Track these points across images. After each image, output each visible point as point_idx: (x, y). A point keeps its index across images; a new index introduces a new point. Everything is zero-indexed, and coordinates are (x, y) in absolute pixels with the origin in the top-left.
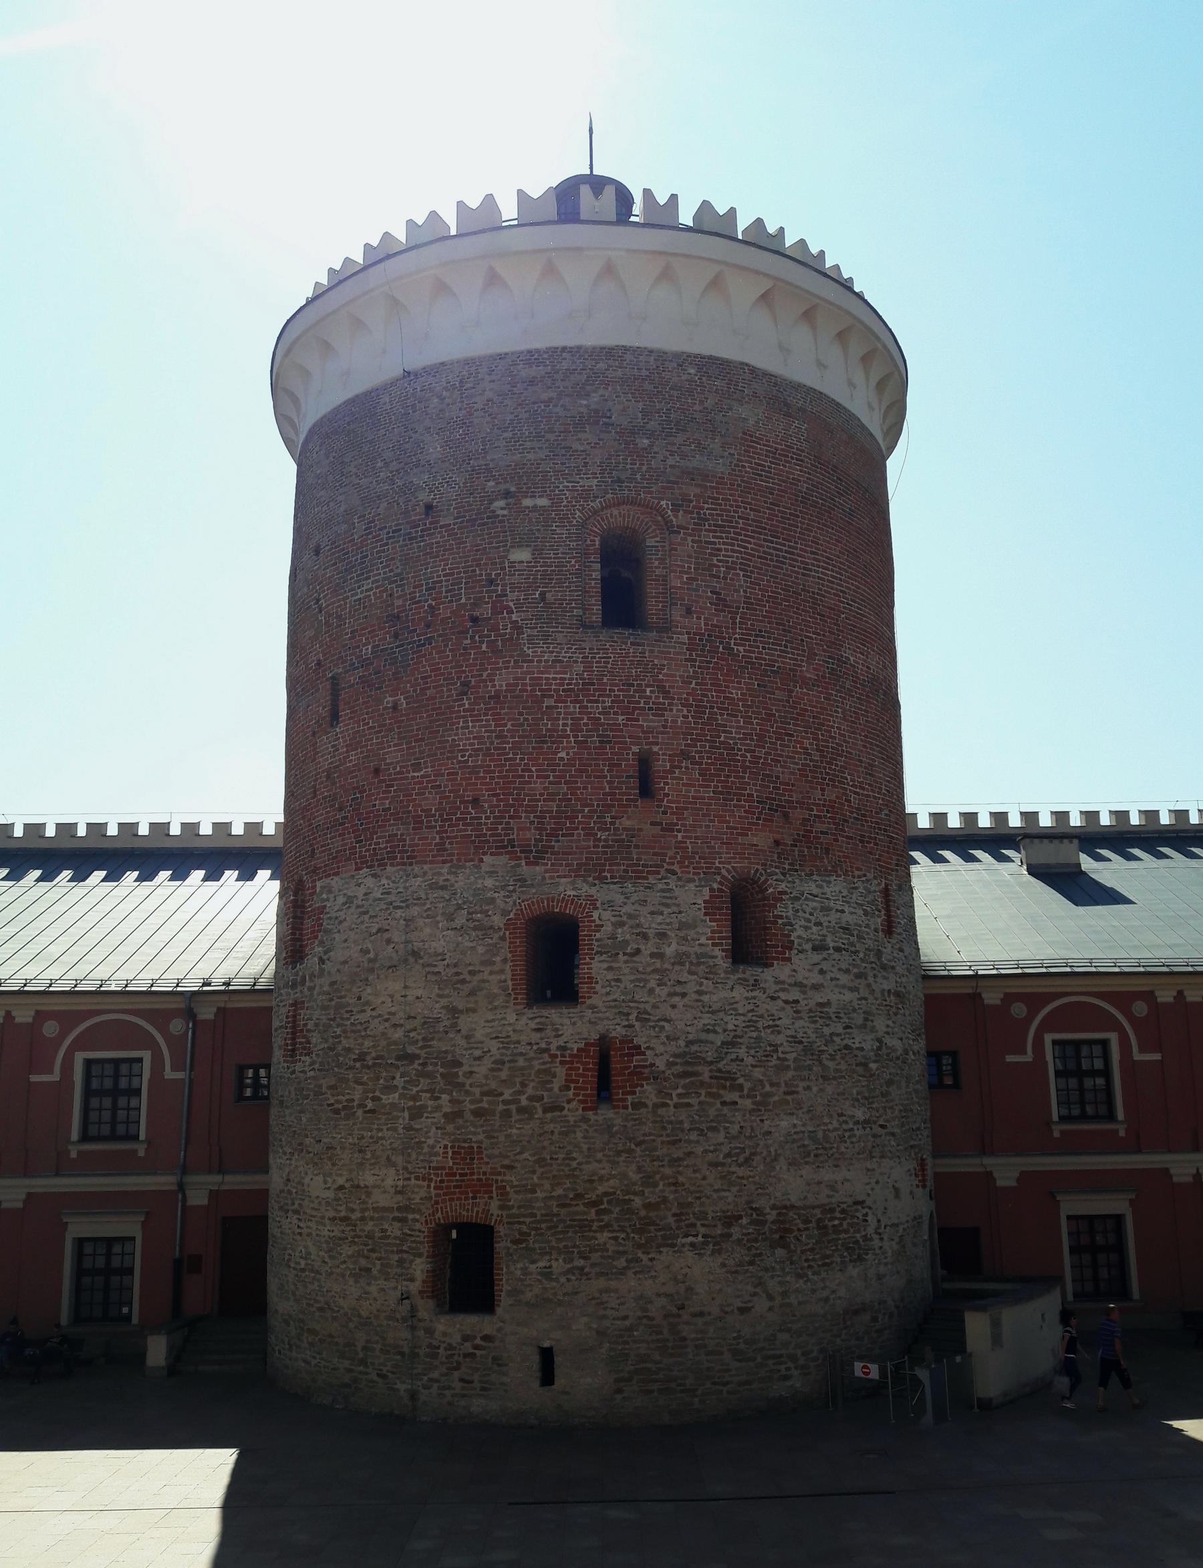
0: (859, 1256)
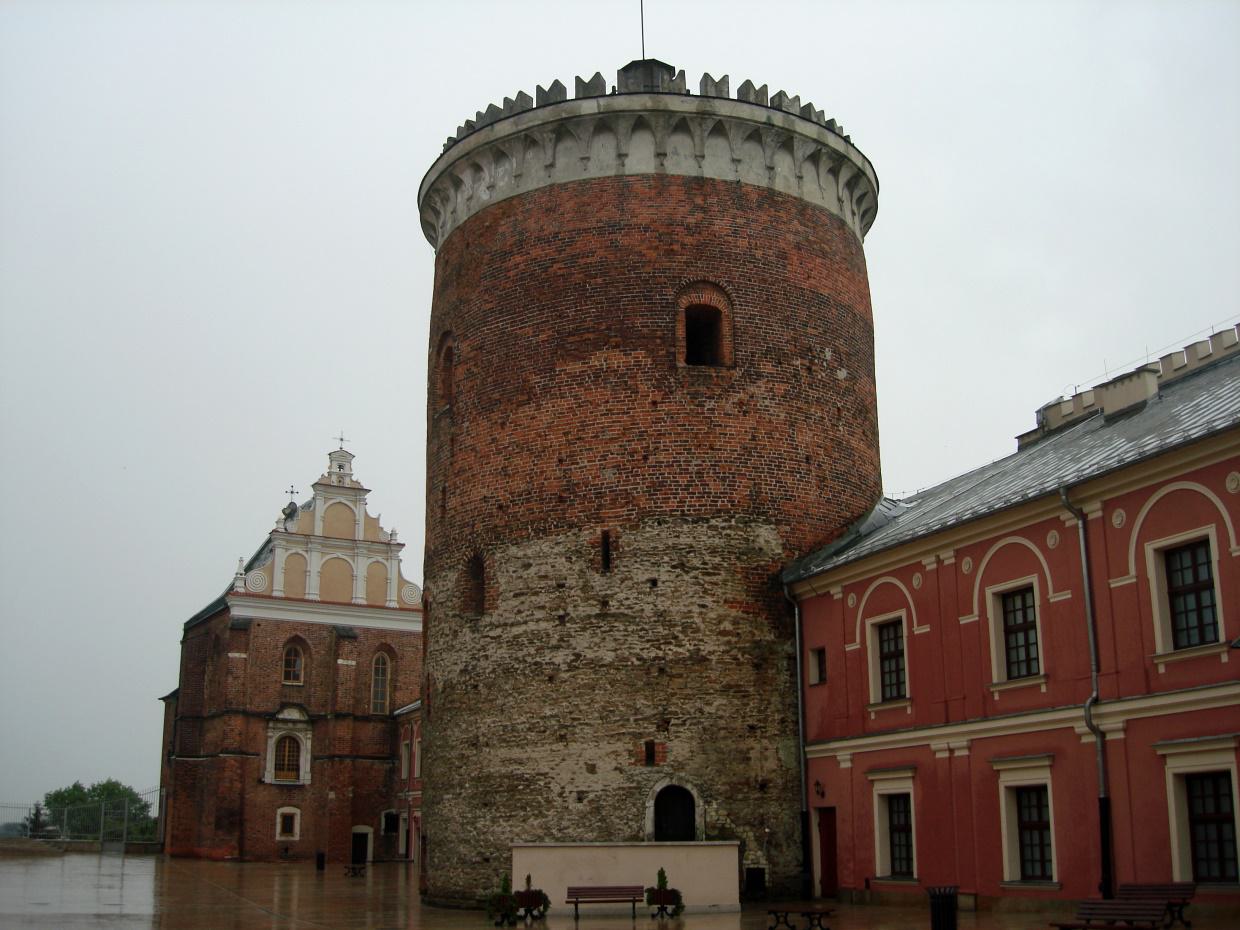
0: (540, 812)
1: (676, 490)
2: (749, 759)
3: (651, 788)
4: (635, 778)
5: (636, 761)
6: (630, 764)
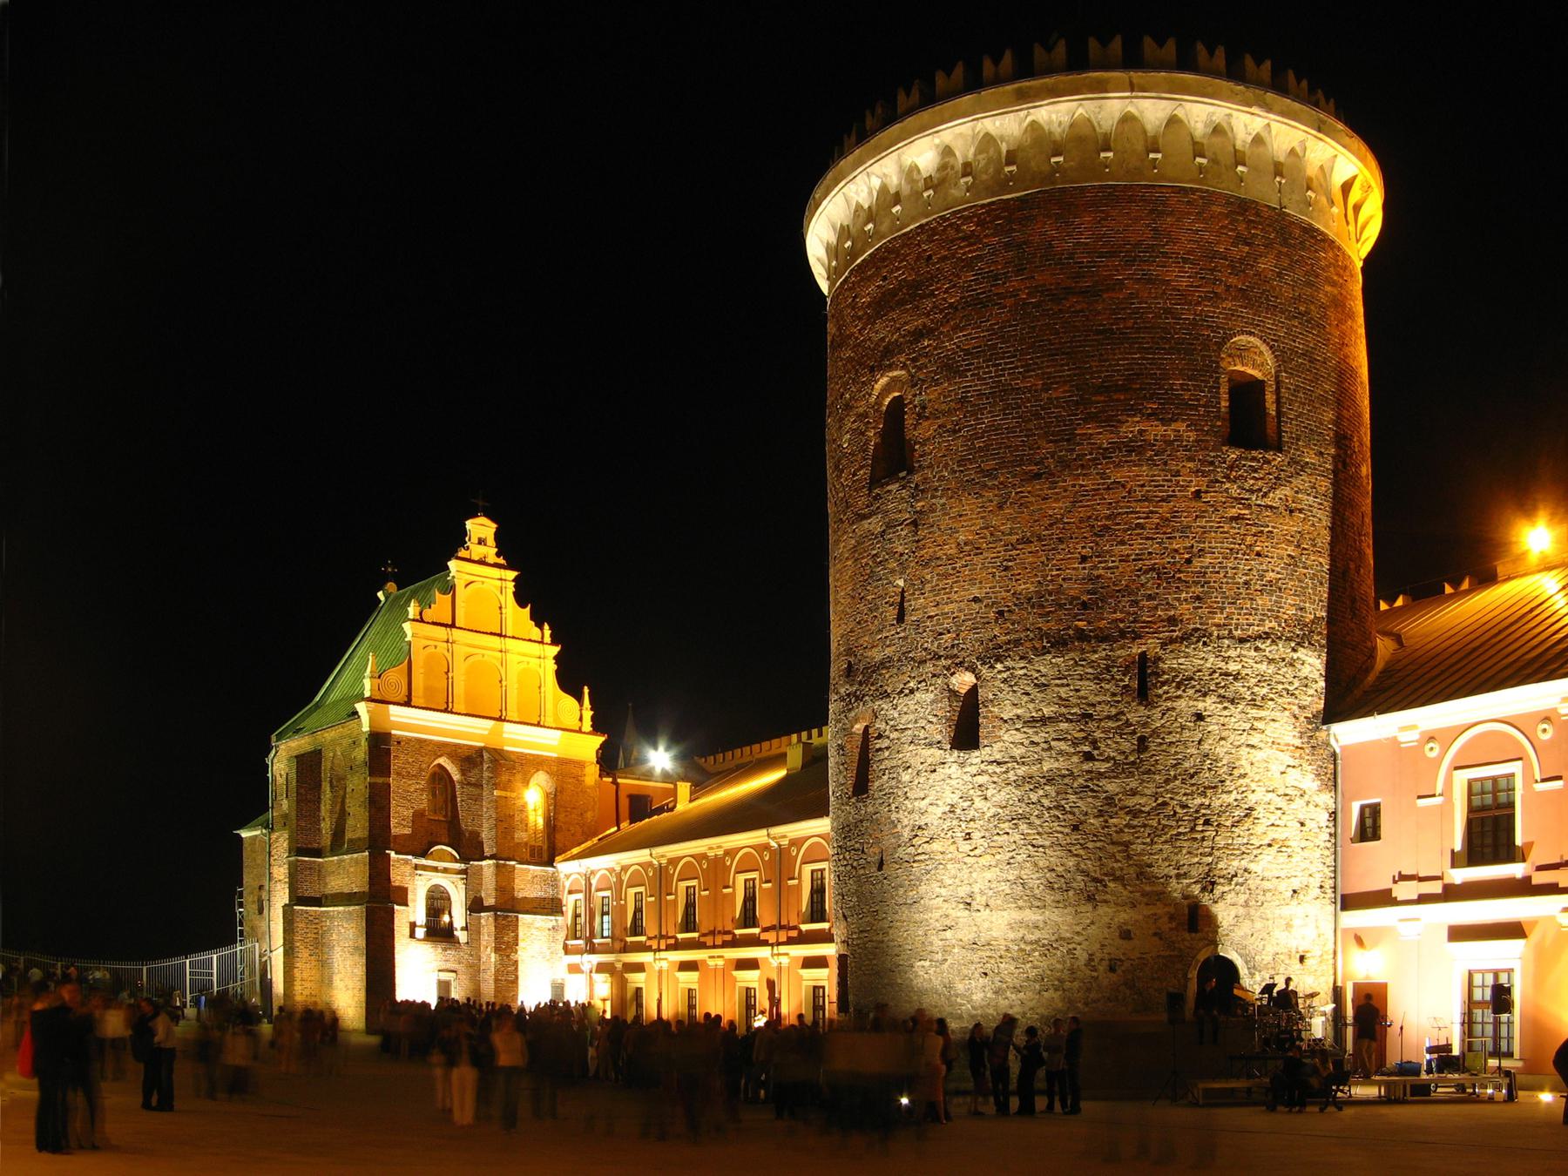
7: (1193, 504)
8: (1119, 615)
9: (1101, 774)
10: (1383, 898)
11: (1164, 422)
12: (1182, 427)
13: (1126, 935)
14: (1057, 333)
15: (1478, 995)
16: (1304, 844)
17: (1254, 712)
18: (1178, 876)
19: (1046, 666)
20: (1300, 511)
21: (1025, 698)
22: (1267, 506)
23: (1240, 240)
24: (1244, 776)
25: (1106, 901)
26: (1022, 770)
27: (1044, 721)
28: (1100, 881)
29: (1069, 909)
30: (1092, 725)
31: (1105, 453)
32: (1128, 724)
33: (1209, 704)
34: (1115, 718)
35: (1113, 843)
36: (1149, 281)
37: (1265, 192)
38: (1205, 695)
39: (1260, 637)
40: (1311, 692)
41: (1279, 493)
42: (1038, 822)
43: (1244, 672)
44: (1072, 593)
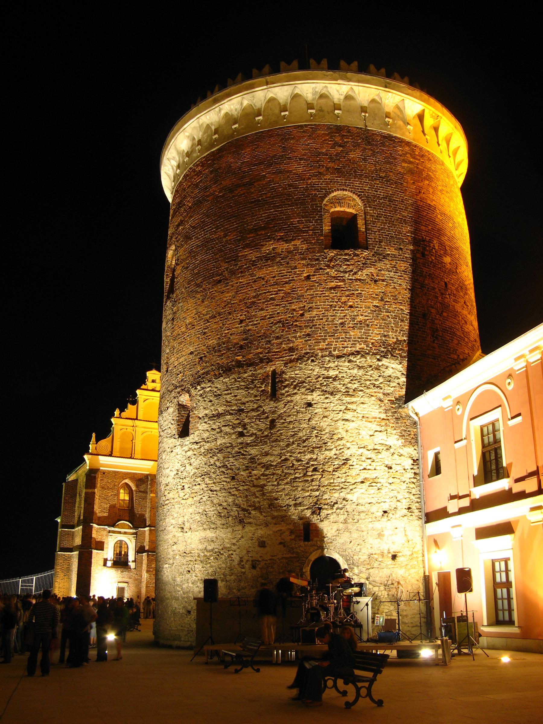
1: (325, 336)
2: (383, 535)
3: (307, 558)
4: (295, 550)
5: (296, 536)
6: (291, 540)
7: (305, 282)
8: (259, 350)
9: (247, 444)
10: (442, 514)
11: (287, 241)
12: (298, 243)
13: (262, 544)
14: (231, 207)
15: (498, 580)
16: (391, 480)
17: (348, 399)
18: (295, 505)
19: (220, 384)
20: (383, 281)
21: (210, 404)
22: (356, 280)
23: (336, 144)
24: (341, 439)
25: (250, 523)
26: (207, 446)
27: (219, 415)
28: (247, 510)
29: (230, 529)
30: (243, 415)
31: (254, 263)
32: (264, 412)
33: (315, 397)
34: (256, 410)
35: (254, 486)
36: (280, 172)
37: (355, 121)
38: (312, 391)
39: (353, 354)
40: (392, 384)
41: (365, 272)
42: (214, 476)
43: (340, 376)
44: (235, 341)
